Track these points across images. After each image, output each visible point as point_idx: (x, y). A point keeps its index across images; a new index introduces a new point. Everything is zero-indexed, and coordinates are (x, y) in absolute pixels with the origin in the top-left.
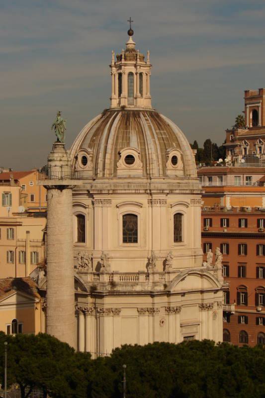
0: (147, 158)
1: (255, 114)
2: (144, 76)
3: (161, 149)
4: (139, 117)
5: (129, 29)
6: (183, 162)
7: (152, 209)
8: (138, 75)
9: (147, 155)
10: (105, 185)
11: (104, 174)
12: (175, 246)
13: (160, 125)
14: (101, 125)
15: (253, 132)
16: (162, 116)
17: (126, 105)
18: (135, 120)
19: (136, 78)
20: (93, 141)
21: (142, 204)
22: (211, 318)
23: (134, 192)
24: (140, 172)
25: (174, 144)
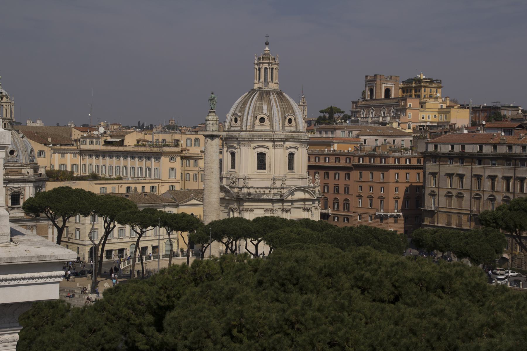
1: (371, 91)
2: (274, 70)
3: (282, 114)
4: (270, 95)
5: (266, 41)
6: (296, 123)
8: (270, 70)
9: (273, 118)
10: (247, 135)
11: (246, 128)
12: (289, 172)
13: (282, 100)
14: (247, 99)
15: (369, 102)
16: (284, 94)
17: (263, 87)
18: (267, 96)
19: (269, 72)
20: (241, 108)
23: (264, 139)
24: (268, 128)
25: (290, 111)
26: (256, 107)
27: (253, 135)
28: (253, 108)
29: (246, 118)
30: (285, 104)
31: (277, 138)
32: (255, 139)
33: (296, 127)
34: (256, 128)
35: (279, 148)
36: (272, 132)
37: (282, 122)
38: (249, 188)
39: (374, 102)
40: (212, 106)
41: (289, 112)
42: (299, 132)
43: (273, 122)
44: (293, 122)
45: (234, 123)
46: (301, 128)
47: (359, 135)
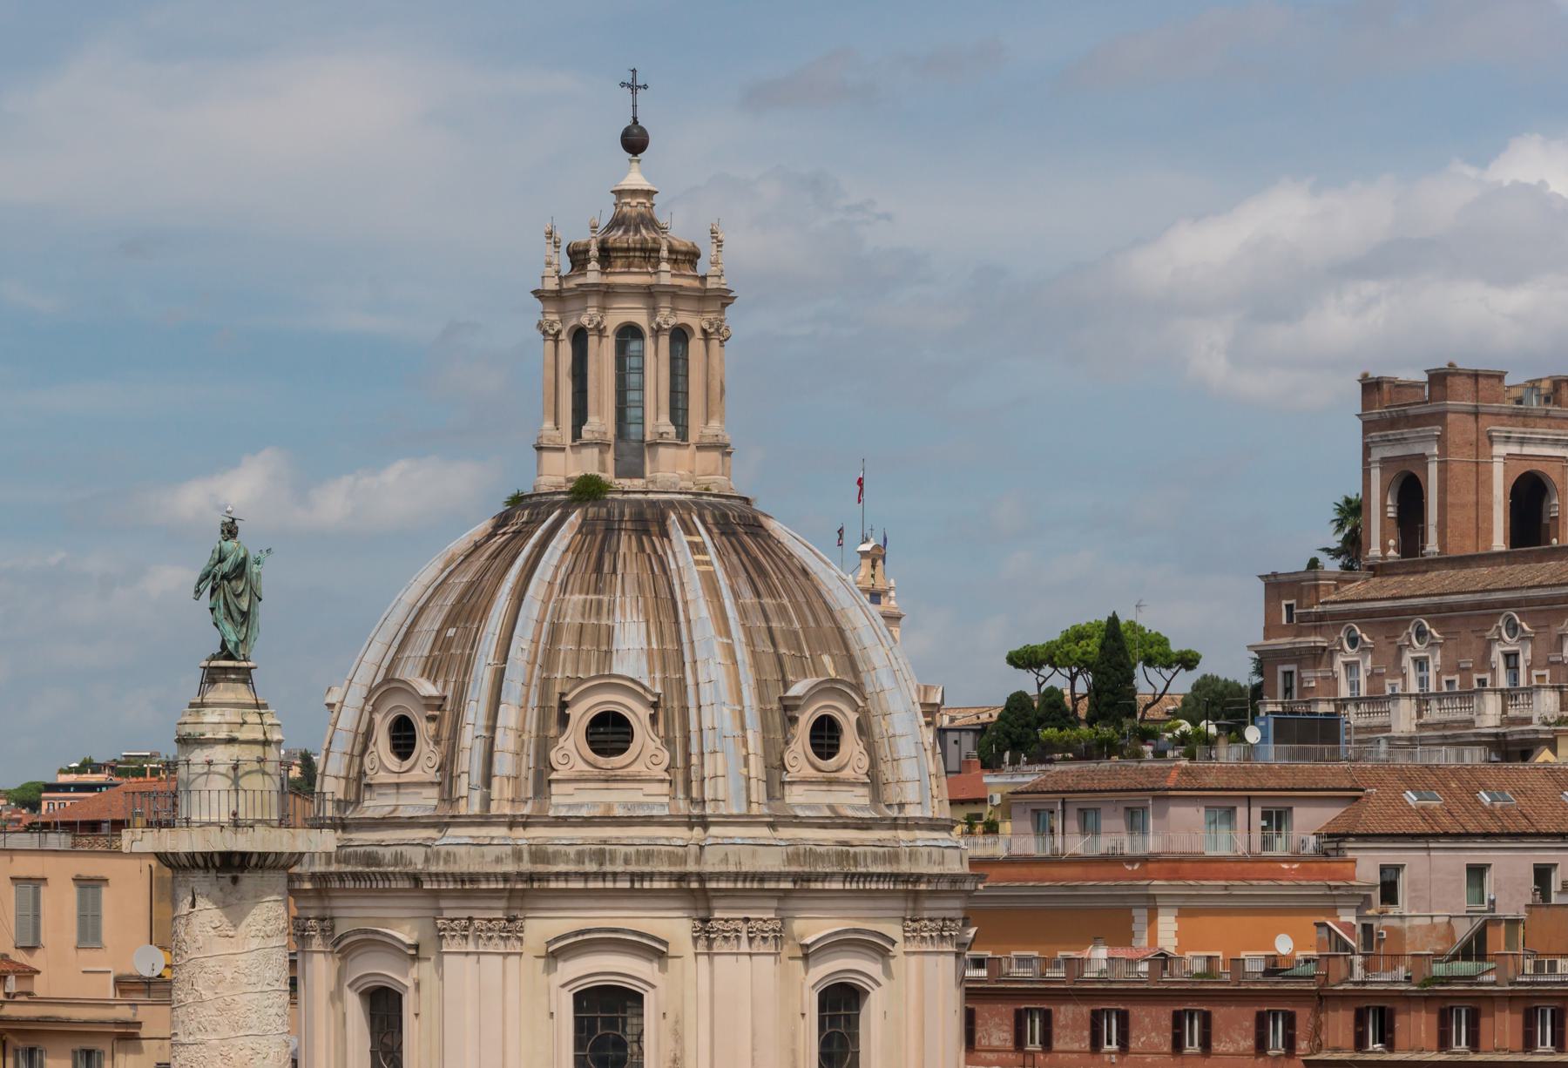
0: (693, 726)
1: (1409, 493)
3: (761, 684)
4: (664, 534)
5: (628, 122)
6: (871, 749)
8: (664, 341)
9: (693, 712)
10: (491, 852)
11: (487, 801)
14: (484, 571)
15: (1392, 585)
16: (775, 526)
17: (608, 476)
18: (642, 549)
19: (655, 359)
21: (665, 943)
24: (655, 797)
25: (826, 659)
26: (555, 632)
27: (539, 855)
28: (535, 641)
29: (482, 721)
30: (782, 610)
31: (732, 869)
32: (553, 885)
33: (874, 782)
34: (562, 799)
35: (745, 947)
36: (691, 826)
37: (767, 743)
39: (1437, 580)
40: (228, 627)
41: (818, 669)
42: (894, 824)
43: (694, 749)
45: (392, 761)
46: (911, 793)
47: (1344, 836)
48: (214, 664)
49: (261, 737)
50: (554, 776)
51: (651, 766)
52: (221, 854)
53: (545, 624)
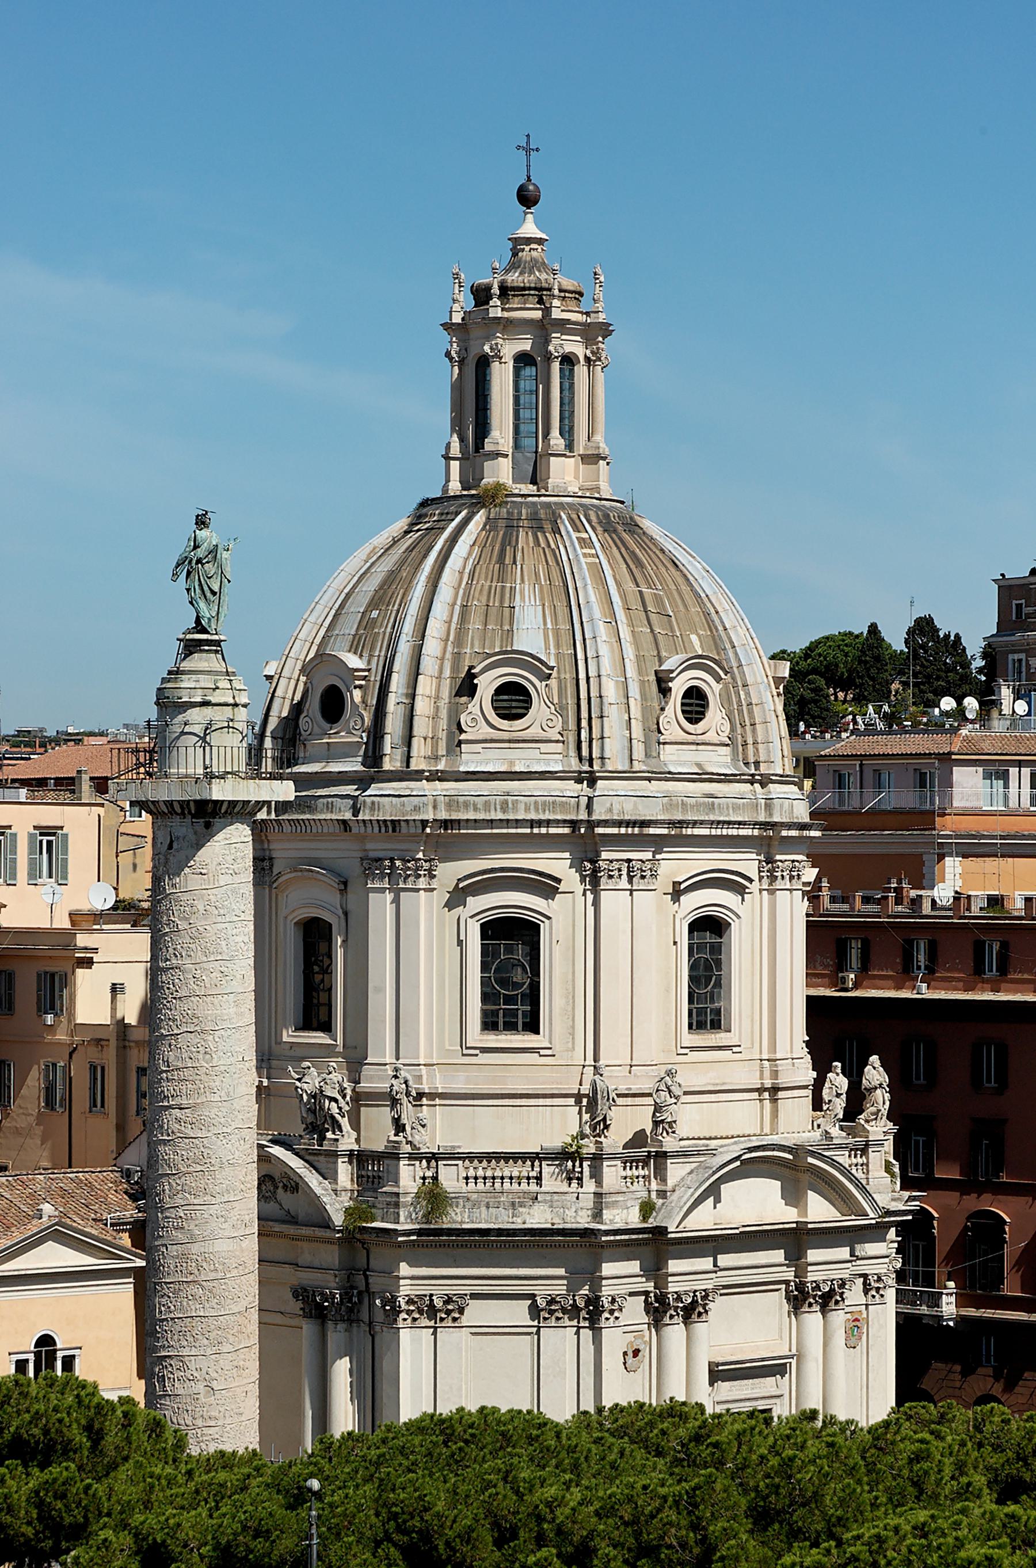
3: (640, 659)
4: (556, 531)
5: (523, 180)
7: (596, 904)
12: (692, 1049)
13: (640, 564)
14: (402, 562)
16: (647, 524)
18: (537, 543)
21: (558, 881)
22: (839, 1338)
27: (452, 802)
29: (403, 690)
35: (624, 883)
36: (579, 781)
37: (645, 710)
38: (434, 1158)
40: (202, 605)
41: (687, 646)
43: (584, 714)
44: (715, 718)
48: (190, 636)
49: (232, 701)
50: (463, 737)
51: (546, 728)
52: (195, 801)
53: (457, 608)
